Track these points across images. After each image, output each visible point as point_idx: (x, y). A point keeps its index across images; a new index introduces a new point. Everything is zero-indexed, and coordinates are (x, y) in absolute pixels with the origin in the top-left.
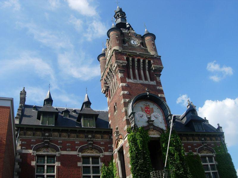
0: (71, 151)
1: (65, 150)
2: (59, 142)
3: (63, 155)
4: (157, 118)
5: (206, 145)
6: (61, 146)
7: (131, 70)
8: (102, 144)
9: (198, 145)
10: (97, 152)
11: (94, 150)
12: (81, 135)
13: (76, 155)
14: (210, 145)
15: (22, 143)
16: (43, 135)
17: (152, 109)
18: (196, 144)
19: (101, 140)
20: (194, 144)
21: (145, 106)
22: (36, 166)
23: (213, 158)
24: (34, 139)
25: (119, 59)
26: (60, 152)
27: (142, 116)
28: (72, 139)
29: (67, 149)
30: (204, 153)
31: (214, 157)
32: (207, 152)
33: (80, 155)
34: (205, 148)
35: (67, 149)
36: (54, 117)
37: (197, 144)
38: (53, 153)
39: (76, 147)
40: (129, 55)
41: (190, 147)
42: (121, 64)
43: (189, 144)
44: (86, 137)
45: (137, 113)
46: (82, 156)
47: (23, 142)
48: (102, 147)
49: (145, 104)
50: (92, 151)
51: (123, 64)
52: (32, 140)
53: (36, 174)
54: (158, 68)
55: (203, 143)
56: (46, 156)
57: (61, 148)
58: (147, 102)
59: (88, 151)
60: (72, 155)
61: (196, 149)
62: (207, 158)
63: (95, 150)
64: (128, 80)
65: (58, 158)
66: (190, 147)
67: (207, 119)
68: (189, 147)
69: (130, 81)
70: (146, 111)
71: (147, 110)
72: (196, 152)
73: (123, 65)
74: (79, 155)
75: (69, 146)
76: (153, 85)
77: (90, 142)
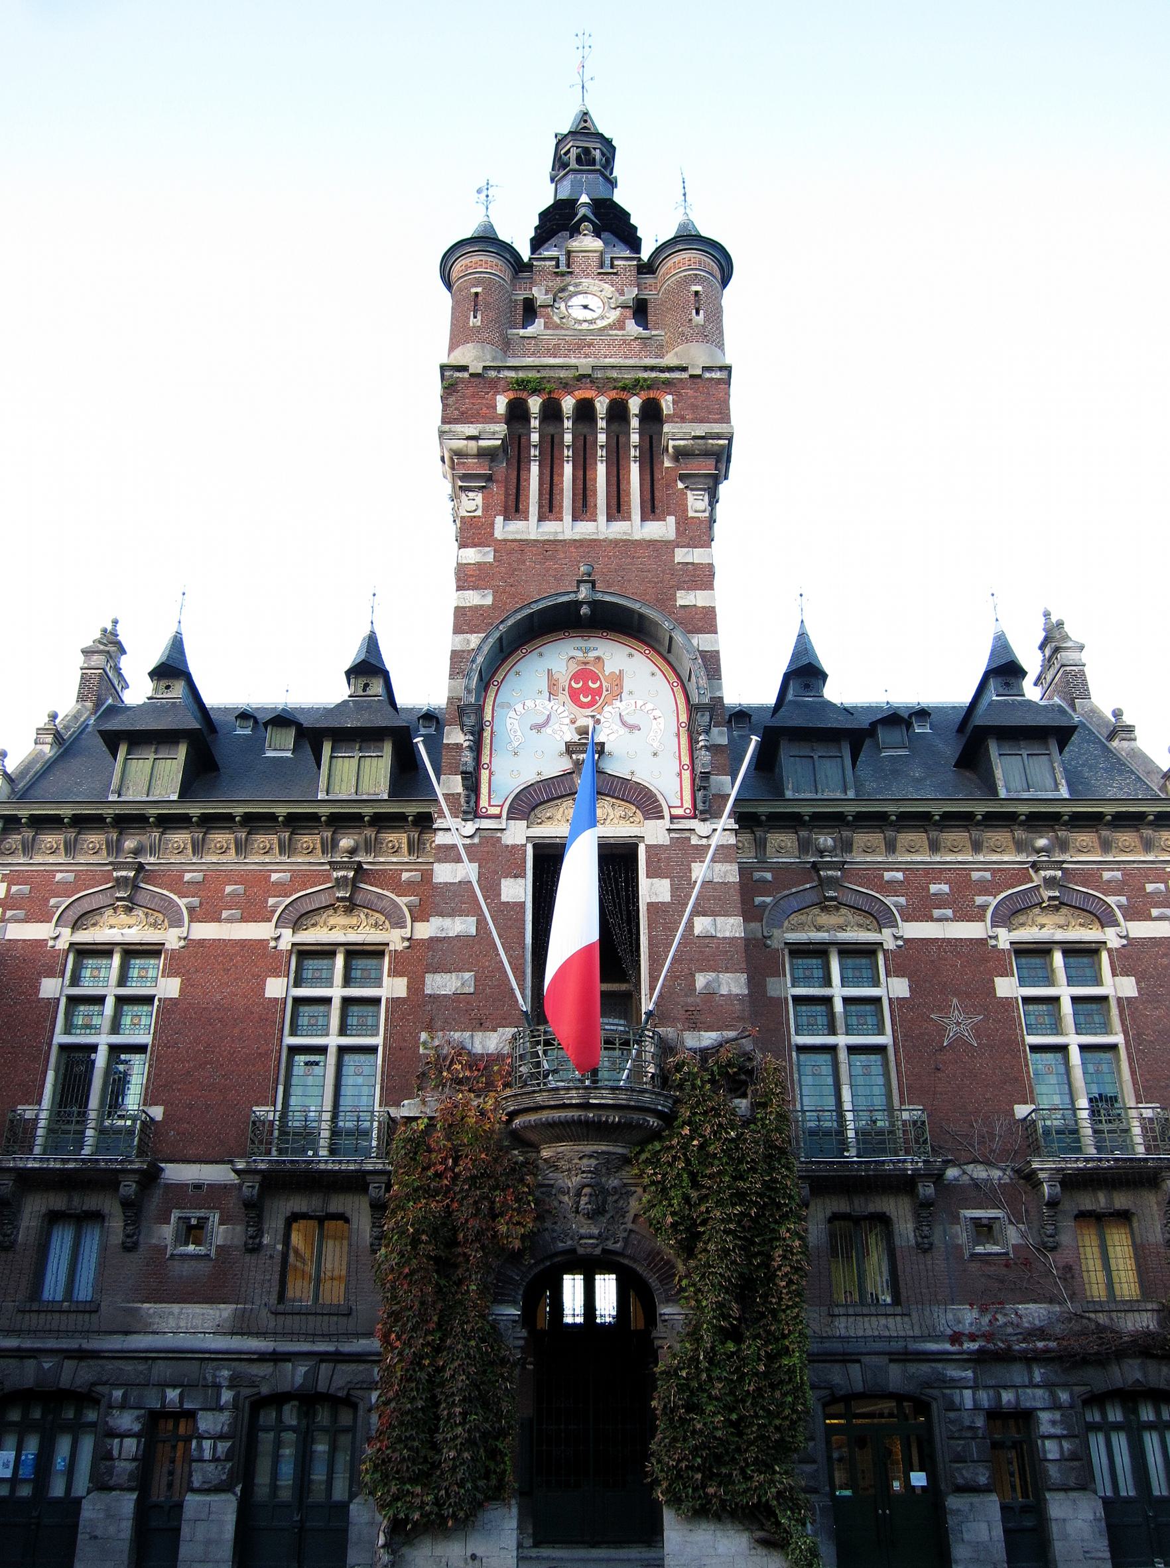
0: (243, 919)
1: (212, 916)
2: (188, 877)
3: (201, 942)
4: (632, 728)
5: (1054, 878)
6: (195, 901)
7: (568, 469)
8: (409, 883)
9: (1002, 878)
10: (376, 925)
11: (363, 916)
12: (306, 838)
13: (262, 943)
14: (1090, 877)
15: (8, 890)
16: (114, 848)
17: (618, 679)
18: (988, 875)
19: (406, 860)
20: (975, 875)
21: (574, 668)
22: (63, 1001)
23: (1104, 956)
24: (67, 871)
25: (464, 418)
26: (182, 932)
27: (549, 717)
28: (255, 860)
29: (225, 914)
30: (1043, 926)
31: (1109, 951)
32: (1062, 921)
33: (288, 938)
34: (1051, 898)
35: (225, 914)
36: (388, 748)
37: (994, 872)
38: (151, 936)
39: (271, 901)
40: (522, 384)
41: (945, 888)
42: (472, 444)
43: (936, 874)
44: (330, 846)
45: (519, 707)
46: (293, 945)
47: (14, 889)
48: (406, 899)
49: (579, 654)
50: (354, 921)
51: (483, 443)
52: (59, 876)
53: (290, 1041)
54: (695, 438)
55: (1035, 866)
56: (118, 948)
57: (191, 910)
58: (593, 642)
59: (332, 921)
60: (243, 944)
61: (980, 900)
62: (1058, 958)
63: (367, 915)
64: (503, 529)
65: (174, 955)
66: (945, 888)
67: (1127, 719)
68: (933, 888)
69: (530, 528)
70: (574, 695)
71: (586, 690)
72: (982, 919)
73: (479, 448)
74: (277, 939)
75: (233, 894)
76: (651, 543)
77: (341, 874)
